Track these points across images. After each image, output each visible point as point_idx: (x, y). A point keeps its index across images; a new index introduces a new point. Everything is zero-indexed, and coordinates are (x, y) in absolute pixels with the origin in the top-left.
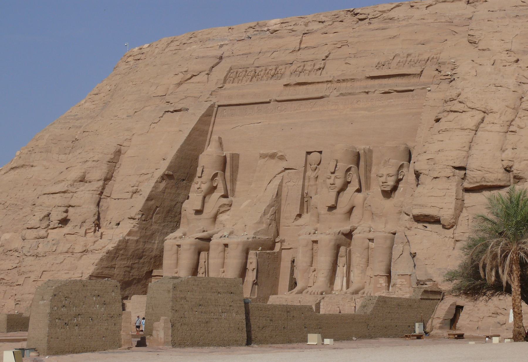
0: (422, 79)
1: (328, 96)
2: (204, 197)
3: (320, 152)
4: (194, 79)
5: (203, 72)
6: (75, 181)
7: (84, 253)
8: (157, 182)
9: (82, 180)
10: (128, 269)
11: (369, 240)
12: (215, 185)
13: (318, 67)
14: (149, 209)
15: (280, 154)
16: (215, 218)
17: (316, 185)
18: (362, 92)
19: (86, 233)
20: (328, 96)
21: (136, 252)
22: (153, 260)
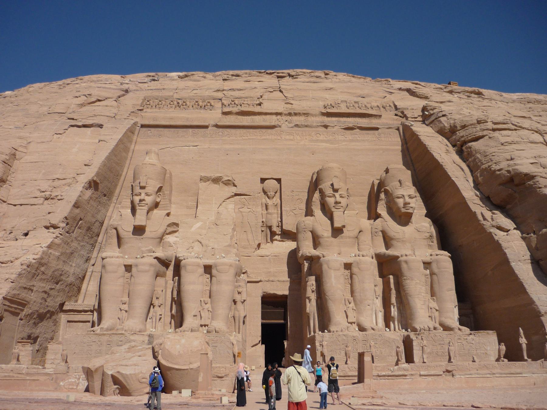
0: (382, 121)
1: (280, 126)
2: (148, 213)
3: (279, 181)
4: (98, 103)
5: (109, 98)
10: (45, 296)
11: (424, 263)
13: (258, 102)
14: (74, 219)
15: (226, 178)
16: (161, 238)
17: (274, 213)
18: (321, 126)
20: (280, 126)
21: (56, 273)
22: (67, 289)
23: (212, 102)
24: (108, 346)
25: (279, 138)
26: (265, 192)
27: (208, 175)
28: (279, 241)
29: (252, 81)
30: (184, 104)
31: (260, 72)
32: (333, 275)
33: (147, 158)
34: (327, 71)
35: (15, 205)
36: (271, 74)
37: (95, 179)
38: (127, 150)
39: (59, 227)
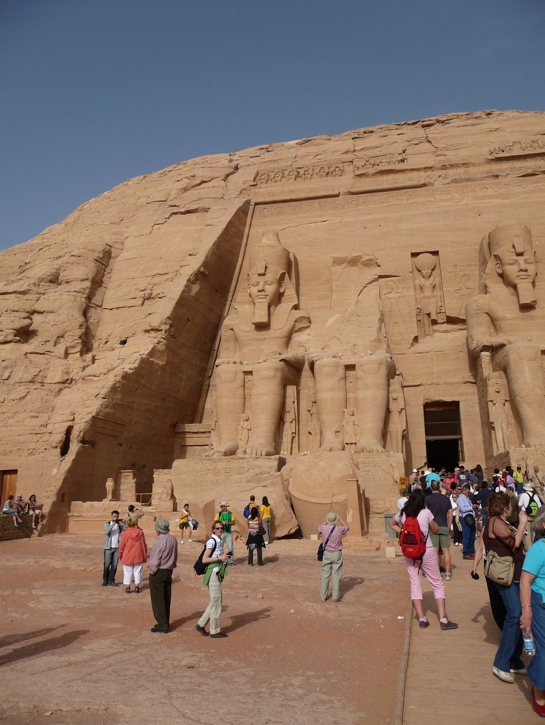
1: (432, 184)
2: (269, 307)
3: (436, 253)
4: (204, 185)
5: (216, 178)
6: (41, 280)
7: (66, 385)
8: (189, 280)
9: (55, 280)
12: (282, 290)
13: (400, 158)
15: (366, 258)
16: (288, 339)
18: (487, 177)
19: (67, 354)
20: (432, 184)
23: (341, 165)
24: (227, 474)
25: (431, 199)
26: (420, 271)
27: (343, 255)
28: (443, 332)
29: (390, 135)
30: (306, 173)
31: (399, 125)
32: (526, 368)
33: (264, 240)
34: (488, 111)
35: (112, 309)
36: (414, 124)
37: (202, 269)
38: (240, 235)
39: (161, 330)
